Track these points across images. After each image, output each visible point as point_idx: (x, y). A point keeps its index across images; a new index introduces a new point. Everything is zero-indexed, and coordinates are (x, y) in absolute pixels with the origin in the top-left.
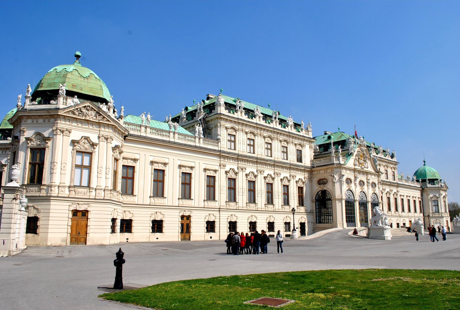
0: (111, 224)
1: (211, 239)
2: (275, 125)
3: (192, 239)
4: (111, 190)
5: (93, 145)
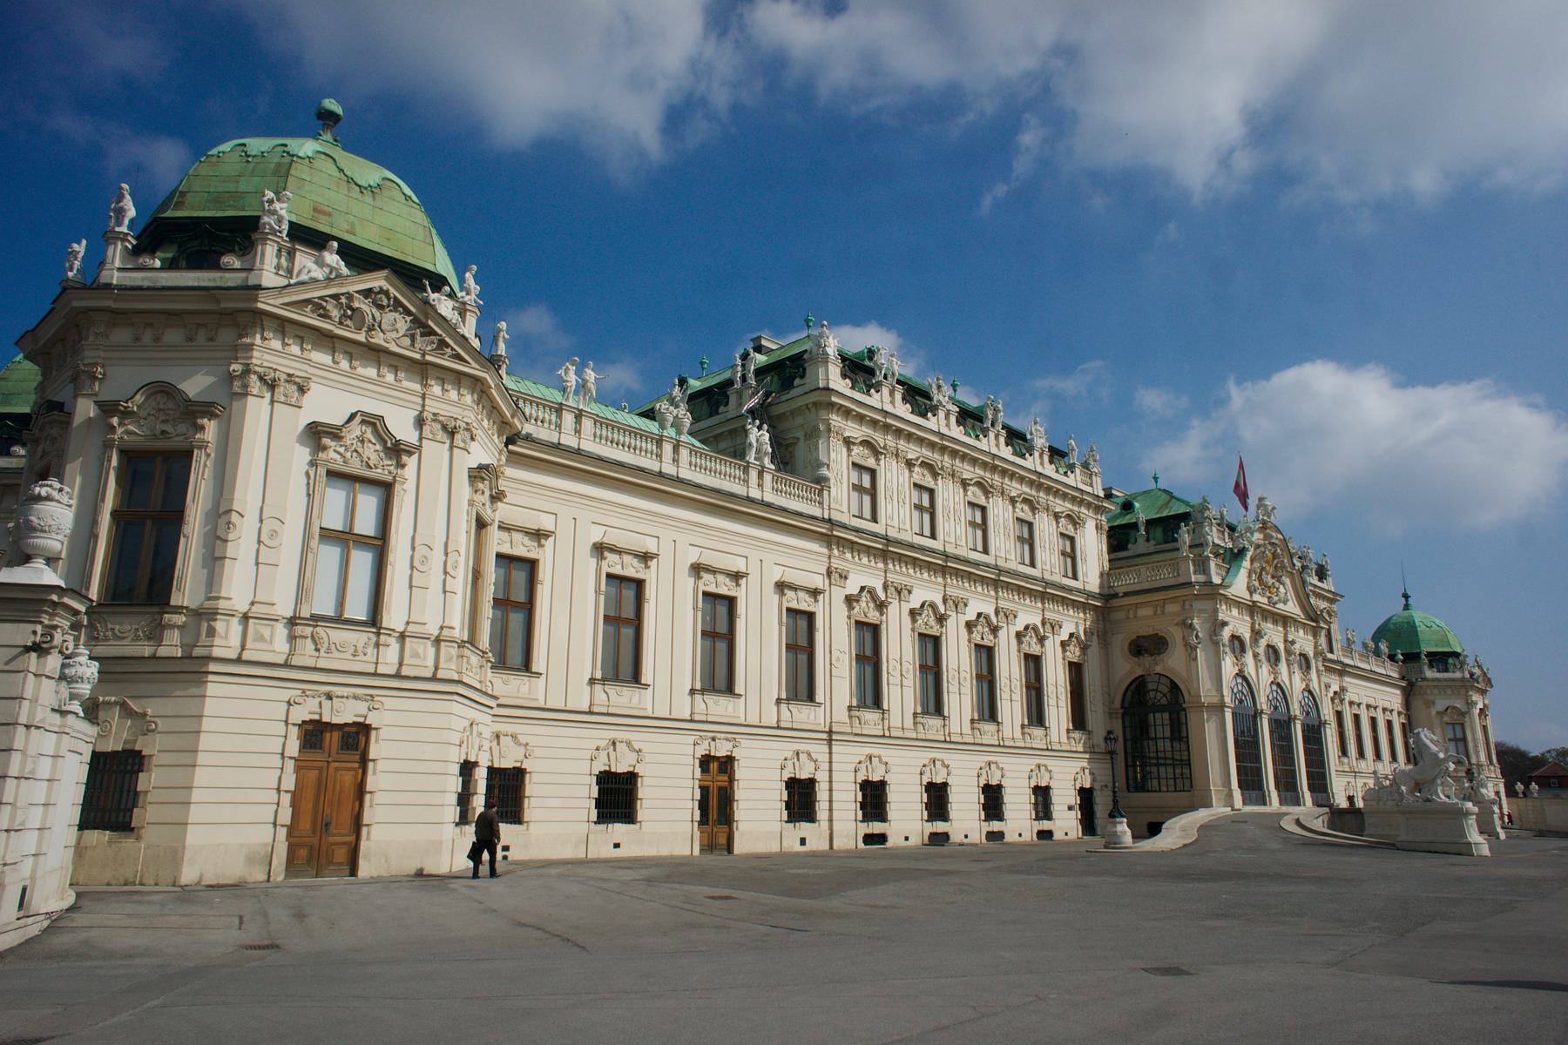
0: (455, 784)
1: (803, 849)
2: (994, 445)
3: (740, 847)
4: (461, 645)
5: (396, 451)
